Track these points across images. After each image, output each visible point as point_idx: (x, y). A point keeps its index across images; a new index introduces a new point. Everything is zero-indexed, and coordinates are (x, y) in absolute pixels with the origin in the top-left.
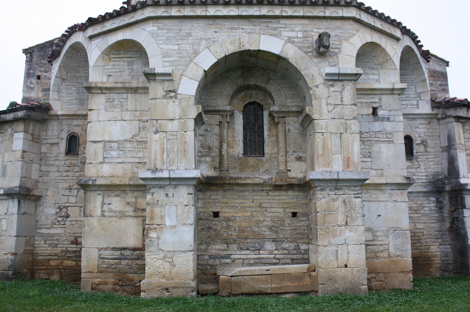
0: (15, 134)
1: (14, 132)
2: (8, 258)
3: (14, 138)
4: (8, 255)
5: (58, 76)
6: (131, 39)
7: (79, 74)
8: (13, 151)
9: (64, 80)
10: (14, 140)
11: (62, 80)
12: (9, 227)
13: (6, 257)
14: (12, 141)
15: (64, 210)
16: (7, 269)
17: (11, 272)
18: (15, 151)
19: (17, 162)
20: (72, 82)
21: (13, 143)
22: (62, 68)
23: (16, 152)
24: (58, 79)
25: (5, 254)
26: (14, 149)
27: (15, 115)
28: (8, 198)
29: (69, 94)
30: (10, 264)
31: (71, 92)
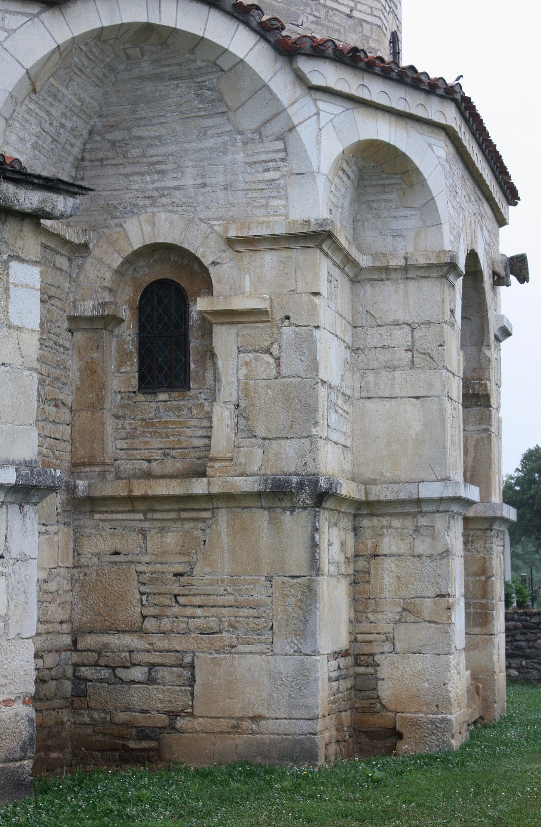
0: (14, 265)
1: (12, 257)
2: (16, 715)
3: (11, 280)
4: (16, 706)
5: (32, 73)
6: (404, 155)
7: (65, 91)
8: (10, 326)
9: (34, 91)
10: (11, 286)
11: (30, 88)
12: (12, 606)
13: (8, 712)
14: (7, 289)
15: (194, 551)
16: (18, 755)
17: (28, 764)
18: (19, 329)
19: (28, 373)
20: (41, 108)
21: (8, 297)
22: (57, 56)
23: (24, 335)
24: (27, 82)
25: (7, 703)
26: (15, 320)
27: (44, 201)
28: (9, 499)
29: (22, 140)
30: (25, 735)
31: (27, 137)
